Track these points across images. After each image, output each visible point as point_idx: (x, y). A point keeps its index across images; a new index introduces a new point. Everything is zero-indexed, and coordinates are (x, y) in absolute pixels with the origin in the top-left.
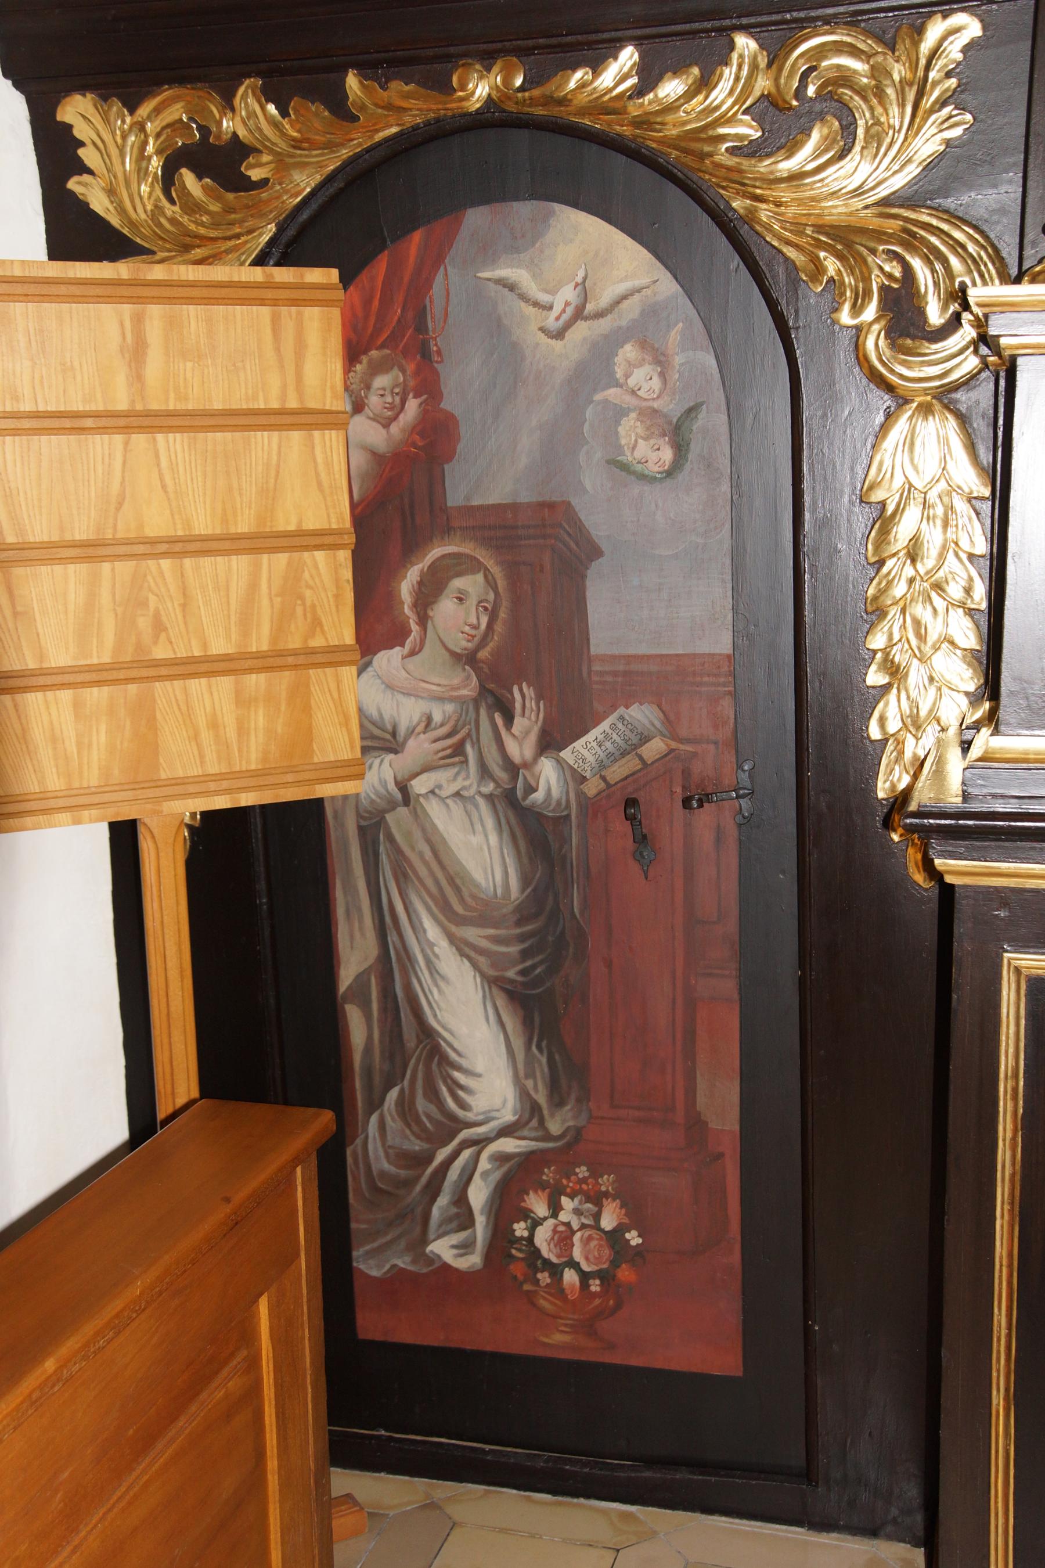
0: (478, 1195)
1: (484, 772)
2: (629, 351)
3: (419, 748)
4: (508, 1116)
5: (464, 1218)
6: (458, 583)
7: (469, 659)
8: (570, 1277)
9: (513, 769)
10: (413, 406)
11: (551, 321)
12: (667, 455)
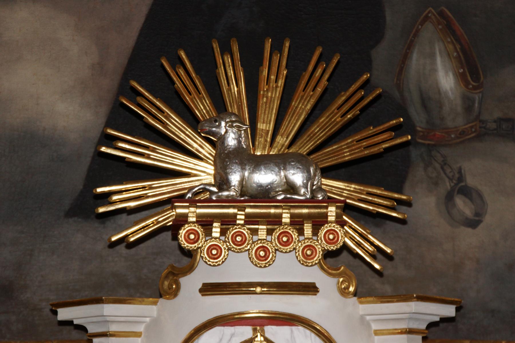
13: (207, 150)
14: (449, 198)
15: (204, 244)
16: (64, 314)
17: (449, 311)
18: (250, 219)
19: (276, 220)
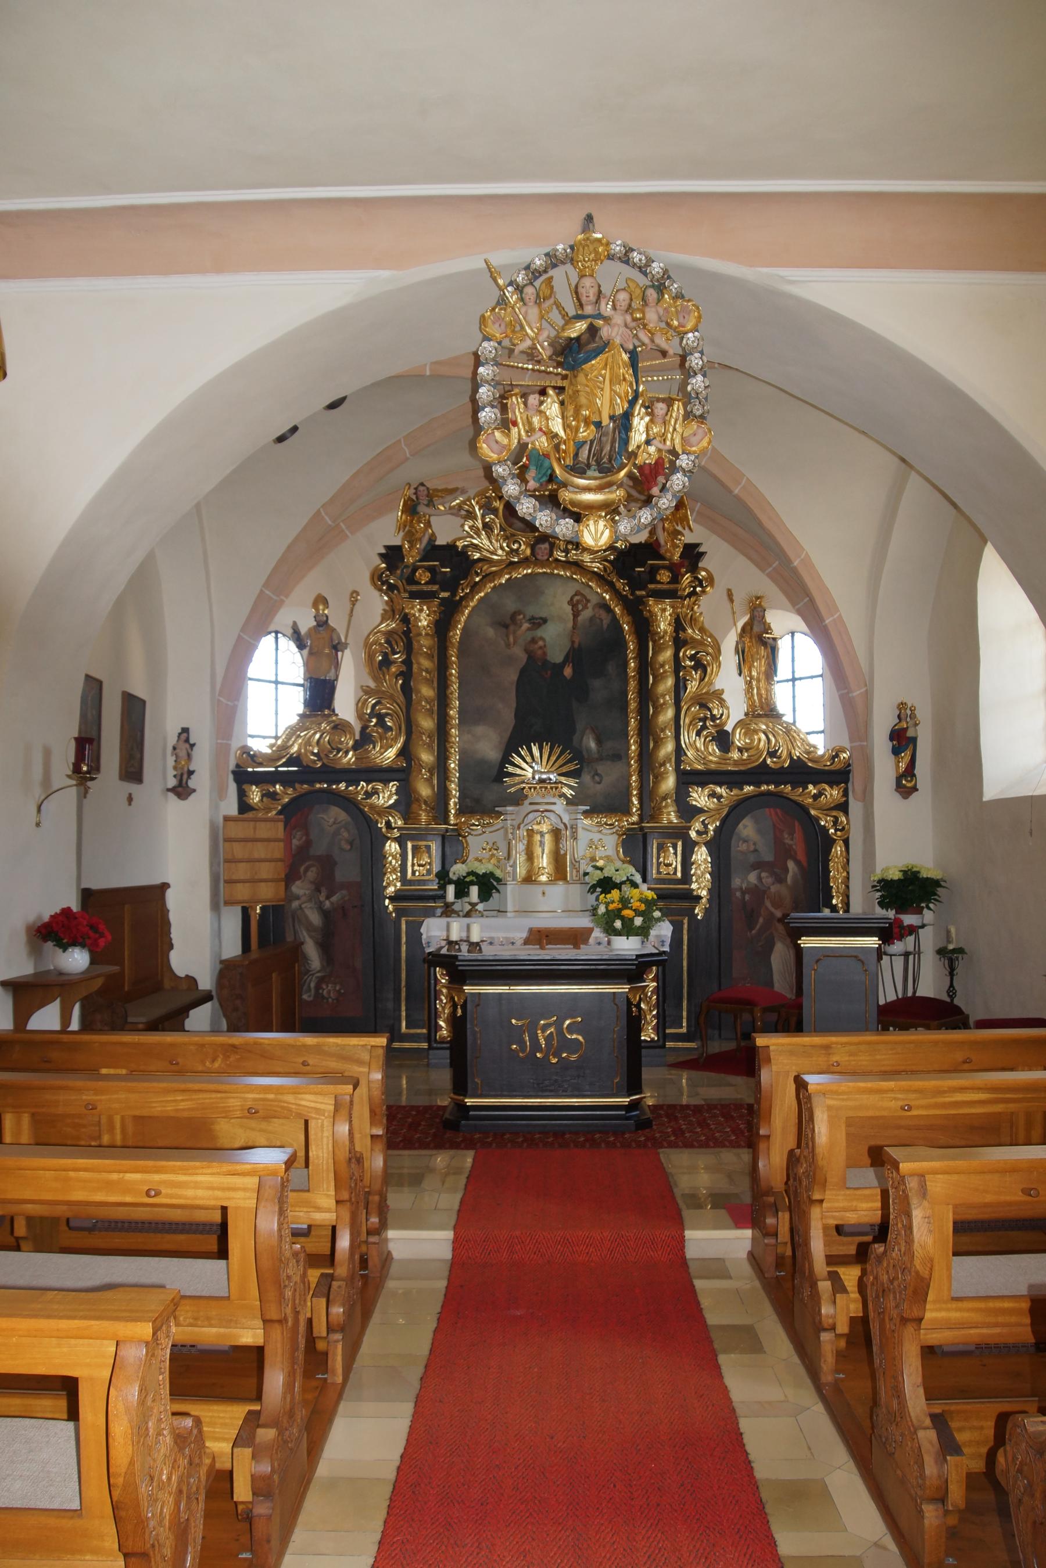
0: (312, 985)
1: (316, 903)
2: (343, 830)
3: (304, 899)
4: (318, 969)
5: (309, 990)
6: (312, 869)
7: (311, 882)
8: (330, 1000)
9: (321, 902)
10: (304, 838)
11: (330, 824)
12: (349, 847)
13: (530, 770)
14: (593, 777)
15: (530, 794)
16: (497, 809)
17: (588, 808)
18: (541, 788)
19: (546, 788)
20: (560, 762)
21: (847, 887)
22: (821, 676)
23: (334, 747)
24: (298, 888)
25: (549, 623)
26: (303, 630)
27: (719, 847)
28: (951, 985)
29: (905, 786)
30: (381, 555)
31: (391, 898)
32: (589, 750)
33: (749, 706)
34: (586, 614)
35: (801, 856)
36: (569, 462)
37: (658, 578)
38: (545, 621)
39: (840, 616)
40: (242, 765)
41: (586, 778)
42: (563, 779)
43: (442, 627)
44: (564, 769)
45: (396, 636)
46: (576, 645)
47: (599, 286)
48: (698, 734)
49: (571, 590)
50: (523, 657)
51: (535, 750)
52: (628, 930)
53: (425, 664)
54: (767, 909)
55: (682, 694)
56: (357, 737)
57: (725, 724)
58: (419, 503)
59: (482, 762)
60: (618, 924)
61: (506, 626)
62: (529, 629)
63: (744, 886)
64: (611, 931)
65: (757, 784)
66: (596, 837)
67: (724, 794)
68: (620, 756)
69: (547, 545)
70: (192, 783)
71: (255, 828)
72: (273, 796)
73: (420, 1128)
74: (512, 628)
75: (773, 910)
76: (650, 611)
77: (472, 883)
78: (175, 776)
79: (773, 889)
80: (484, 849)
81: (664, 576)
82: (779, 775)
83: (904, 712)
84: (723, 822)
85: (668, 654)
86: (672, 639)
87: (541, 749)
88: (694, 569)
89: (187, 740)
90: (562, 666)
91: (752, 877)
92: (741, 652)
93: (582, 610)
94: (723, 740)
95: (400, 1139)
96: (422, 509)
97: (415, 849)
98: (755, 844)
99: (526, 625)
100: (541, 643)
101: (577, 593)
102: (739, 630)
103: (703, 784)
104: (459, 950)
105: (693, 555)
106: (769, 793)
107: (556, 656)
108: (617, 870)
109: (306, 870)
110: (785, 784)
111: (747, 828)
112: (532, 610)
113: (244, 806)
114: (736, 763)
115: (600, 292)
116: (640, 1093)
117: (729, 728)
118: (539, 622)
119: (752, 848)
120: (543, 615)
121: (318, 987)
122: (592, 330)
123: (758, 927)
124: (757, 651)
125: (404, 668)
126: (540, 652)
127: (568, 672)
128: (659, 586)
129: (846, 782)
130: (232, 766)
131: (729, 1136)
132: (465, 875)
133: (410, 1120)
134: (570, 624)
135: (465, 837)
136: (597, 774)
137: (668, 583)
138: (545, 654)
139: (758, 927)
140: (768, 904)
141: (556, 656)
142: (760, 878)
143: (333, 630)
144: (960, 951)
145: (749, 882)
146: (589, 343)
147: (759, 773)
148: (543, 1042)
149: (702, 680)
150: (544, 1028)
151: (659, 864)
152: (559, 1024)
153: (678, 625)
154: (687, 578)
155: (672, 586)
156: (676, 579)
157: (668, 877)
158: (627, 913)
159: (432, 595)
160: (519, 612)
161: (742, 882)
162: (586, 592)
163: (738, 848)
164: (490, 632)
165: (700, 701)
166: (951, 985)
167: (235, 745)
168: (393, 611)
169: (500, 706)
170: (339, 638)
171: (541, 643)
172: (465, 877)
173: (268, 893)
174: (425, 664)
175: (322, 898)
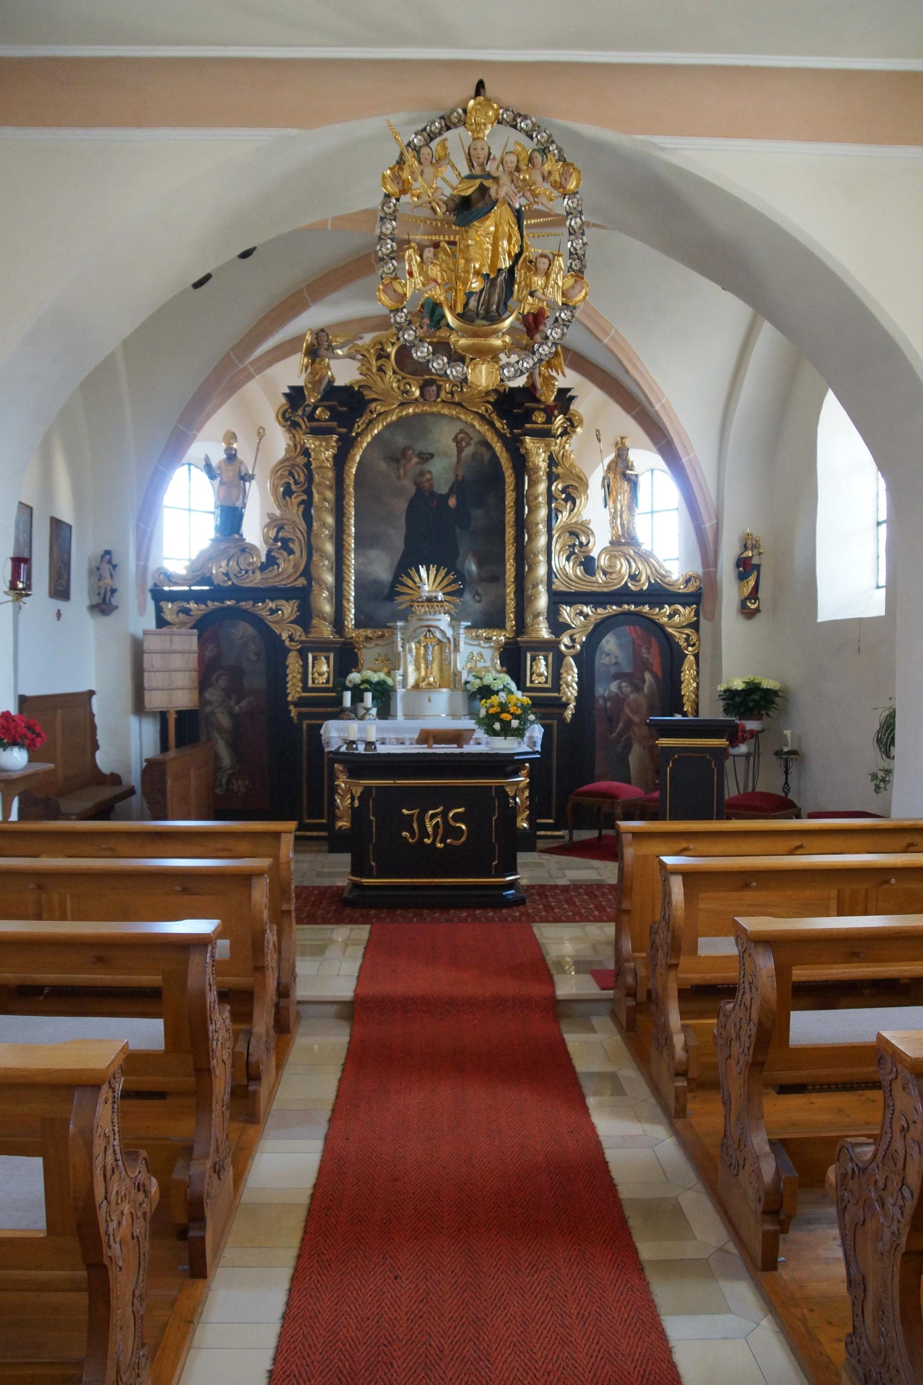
0: (224, 781)
4: (228, 767)
5: (221, 786)
7: (223, 690)
17: (469, 624)
20: (445, 582)
21: (697, 696)
22: (677, 509)
23: (242, 568)
24: (210, 695)
25: (435, 458)
26: (214, 463)
27: (585, 660)
28: (786, 783)
29: (749, 608)
30: (285, 395)
31: (296, 704)
32: (470, 572)
33: (613, 535)
34: (468, 451)
35: (657, 668)
36: (459, 310)
37: (534, 418)
38: (432, 456)
39: (695, 455)
40: (158, 584)
41: (468, 597)
42: (449, 598)
43: (340, 461)
44: (449, 589)
45: (297, 468)
46: (460, 478)
47: (489, 148)
48: (568, 559)
49: (455, 428)
50: (412, 489)
51: (423, 571)
52: (507, 731)
53: (323, 497)
54: (627, 715)
55: (554, 521)
56: (264, 559)
57: (590, 551)
58: (319, 348)
59: (376, 582)
60: (497, 726)
61: (397, 461)
62: (418, 463)
63: (606, 694)
64: (492, 732)
65: (619, 604)
66: (476, 650)
67: (590, 613)
68: (497, 578)
69: (434, 388)
70: (114, 601)
71: (171, 641)
72: (187, 612)
73: (322, 906)
74: (402, 462)
75: (631, 715)
76: (526, 449)
77: (367, 690)
78: (99, 594)
79: (632, 697)
80: (377, 660)
81: (540, 417)
82: (639, 597)
83: (748, 543)
84: (589, 637)
85: (542, 487)
86: (545, 474)
87: (428, 570)
88: (565, 410)
89: (110, 562)
90: (446, 497)
91: (614, 687)
92: (607, 487)
93: (466, 446)
94: (588, 565)
95: (305, 915)
96: (322, 352)
97: (314, 659)
98: (616, 657)
99: (415, 460)
100: (428, 476)
101: (462, 431)
102: (605, 467)
103: (570, 604)
104: (356, 749)
105: (565, 398)
106: (630, 613)
107: (443, 488)
108: (495, 680)
109: (217, 680)
110: (644, 604)
111: (609, 643)
112: (420, 446)
113: (161, 622)
114: (600, 585)
115: (490, 154)
116: (516, 874)
117: (594, 554)
118: (426, 457)
119: (614, 661)
120: (431, 450)
121: (229, 782)
122: (483, 190)
123: (618, 730)
124: (621, 485)
125: (305, 497)
126: (427, 485)
127: (452, 502)
128: (535, 426)
129: (698, 604)
130: (150, 584)
131: (593, 912)
132: (359, 683)
133: (313, 899)
134: (455, 459)
135: (359, 649)
136: (478, 594)
137: (543, 423)
138: (432, 485)
139: (618, 730)
140: (627, 710)
141: (443, 489)
142: (620, 687)
143: (242, 463)
144: (794, 752)
145: (609, 690)
146: (479, 201)
147: (622, 595)
148: (430, 830)
149: (572, 510)
150: (433, 816)
151: (532, 674)
152: (444, 814)
153: (552, 461)
154: (559, 420)
155: (546, 426)
156: (550, 420)
157: (540, 685)
158: (506, 716)
159: (331, 431)
160: (409, 448)
161: (605, 691)
162: (469, 430)
163: (602, 661)
164: (383, 465)
165: (570, 529)
166: (786, 783)
167: (152, 566)
168: (296, 446)
169: (391, 532)
170: (247, 469)
171: (428, 476)
172: (360, 685)
173: (184, 699)
174: (323, 497)
175: (232, 703)
